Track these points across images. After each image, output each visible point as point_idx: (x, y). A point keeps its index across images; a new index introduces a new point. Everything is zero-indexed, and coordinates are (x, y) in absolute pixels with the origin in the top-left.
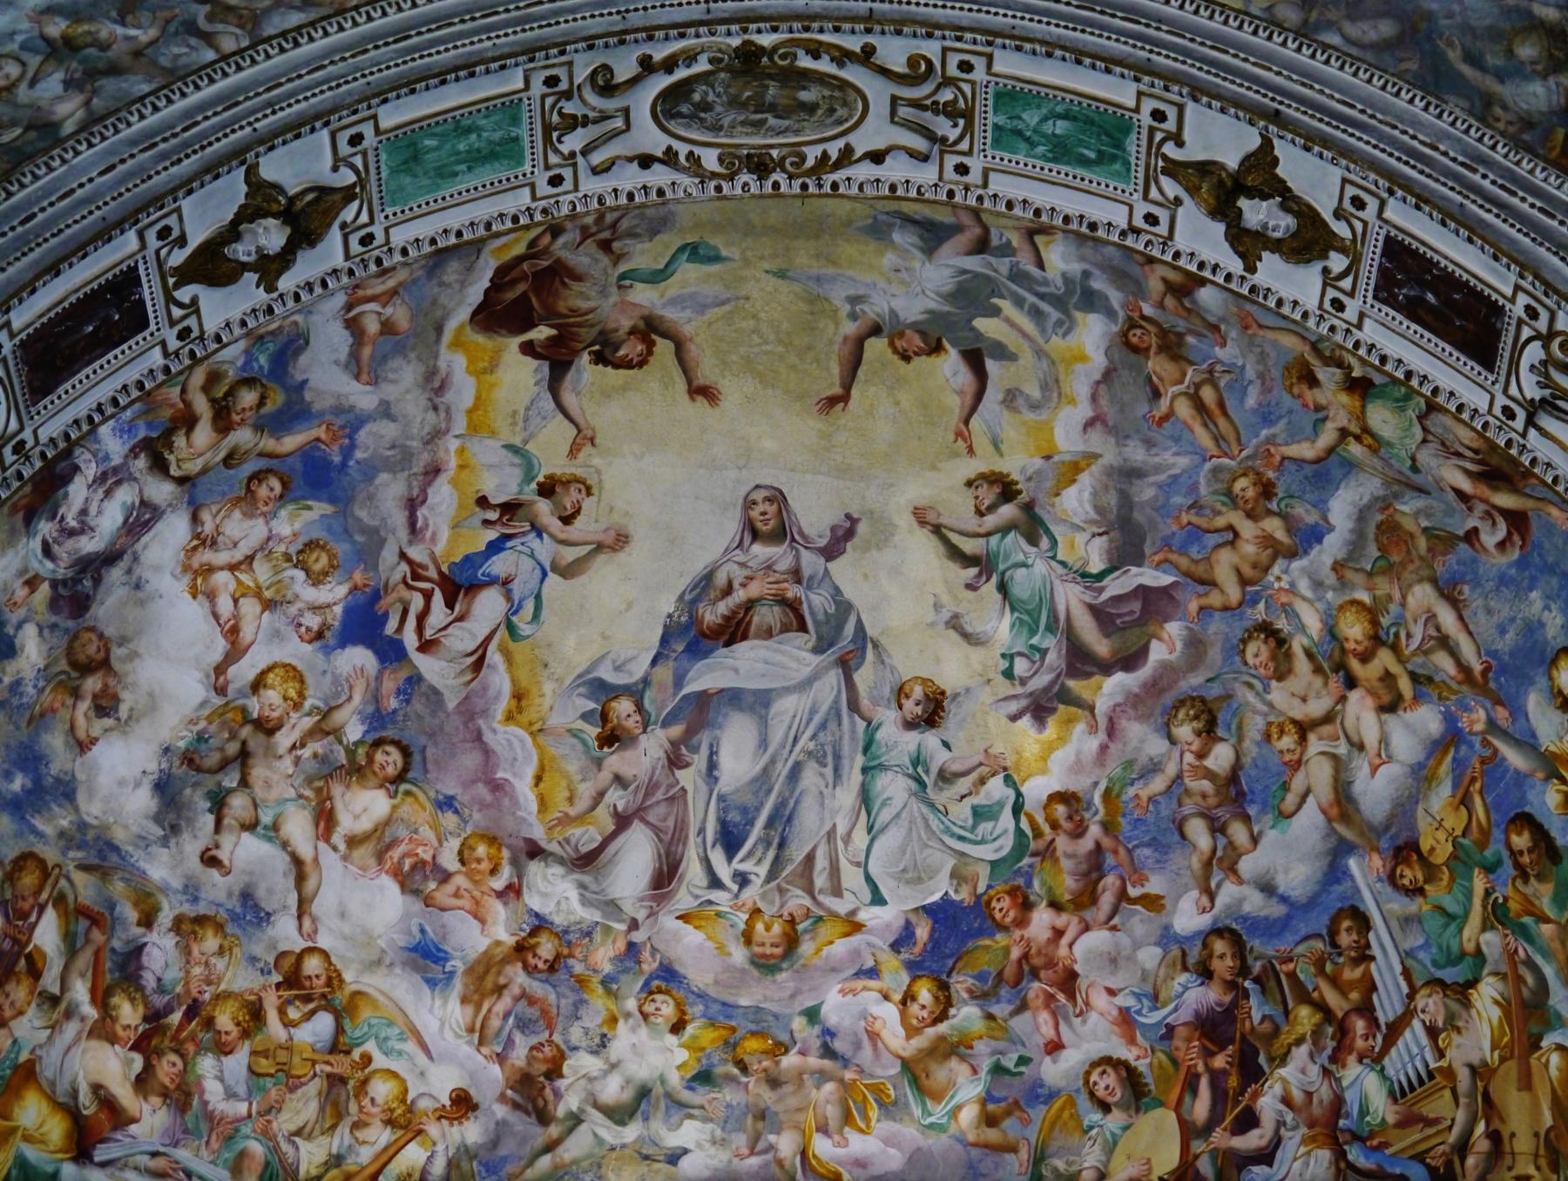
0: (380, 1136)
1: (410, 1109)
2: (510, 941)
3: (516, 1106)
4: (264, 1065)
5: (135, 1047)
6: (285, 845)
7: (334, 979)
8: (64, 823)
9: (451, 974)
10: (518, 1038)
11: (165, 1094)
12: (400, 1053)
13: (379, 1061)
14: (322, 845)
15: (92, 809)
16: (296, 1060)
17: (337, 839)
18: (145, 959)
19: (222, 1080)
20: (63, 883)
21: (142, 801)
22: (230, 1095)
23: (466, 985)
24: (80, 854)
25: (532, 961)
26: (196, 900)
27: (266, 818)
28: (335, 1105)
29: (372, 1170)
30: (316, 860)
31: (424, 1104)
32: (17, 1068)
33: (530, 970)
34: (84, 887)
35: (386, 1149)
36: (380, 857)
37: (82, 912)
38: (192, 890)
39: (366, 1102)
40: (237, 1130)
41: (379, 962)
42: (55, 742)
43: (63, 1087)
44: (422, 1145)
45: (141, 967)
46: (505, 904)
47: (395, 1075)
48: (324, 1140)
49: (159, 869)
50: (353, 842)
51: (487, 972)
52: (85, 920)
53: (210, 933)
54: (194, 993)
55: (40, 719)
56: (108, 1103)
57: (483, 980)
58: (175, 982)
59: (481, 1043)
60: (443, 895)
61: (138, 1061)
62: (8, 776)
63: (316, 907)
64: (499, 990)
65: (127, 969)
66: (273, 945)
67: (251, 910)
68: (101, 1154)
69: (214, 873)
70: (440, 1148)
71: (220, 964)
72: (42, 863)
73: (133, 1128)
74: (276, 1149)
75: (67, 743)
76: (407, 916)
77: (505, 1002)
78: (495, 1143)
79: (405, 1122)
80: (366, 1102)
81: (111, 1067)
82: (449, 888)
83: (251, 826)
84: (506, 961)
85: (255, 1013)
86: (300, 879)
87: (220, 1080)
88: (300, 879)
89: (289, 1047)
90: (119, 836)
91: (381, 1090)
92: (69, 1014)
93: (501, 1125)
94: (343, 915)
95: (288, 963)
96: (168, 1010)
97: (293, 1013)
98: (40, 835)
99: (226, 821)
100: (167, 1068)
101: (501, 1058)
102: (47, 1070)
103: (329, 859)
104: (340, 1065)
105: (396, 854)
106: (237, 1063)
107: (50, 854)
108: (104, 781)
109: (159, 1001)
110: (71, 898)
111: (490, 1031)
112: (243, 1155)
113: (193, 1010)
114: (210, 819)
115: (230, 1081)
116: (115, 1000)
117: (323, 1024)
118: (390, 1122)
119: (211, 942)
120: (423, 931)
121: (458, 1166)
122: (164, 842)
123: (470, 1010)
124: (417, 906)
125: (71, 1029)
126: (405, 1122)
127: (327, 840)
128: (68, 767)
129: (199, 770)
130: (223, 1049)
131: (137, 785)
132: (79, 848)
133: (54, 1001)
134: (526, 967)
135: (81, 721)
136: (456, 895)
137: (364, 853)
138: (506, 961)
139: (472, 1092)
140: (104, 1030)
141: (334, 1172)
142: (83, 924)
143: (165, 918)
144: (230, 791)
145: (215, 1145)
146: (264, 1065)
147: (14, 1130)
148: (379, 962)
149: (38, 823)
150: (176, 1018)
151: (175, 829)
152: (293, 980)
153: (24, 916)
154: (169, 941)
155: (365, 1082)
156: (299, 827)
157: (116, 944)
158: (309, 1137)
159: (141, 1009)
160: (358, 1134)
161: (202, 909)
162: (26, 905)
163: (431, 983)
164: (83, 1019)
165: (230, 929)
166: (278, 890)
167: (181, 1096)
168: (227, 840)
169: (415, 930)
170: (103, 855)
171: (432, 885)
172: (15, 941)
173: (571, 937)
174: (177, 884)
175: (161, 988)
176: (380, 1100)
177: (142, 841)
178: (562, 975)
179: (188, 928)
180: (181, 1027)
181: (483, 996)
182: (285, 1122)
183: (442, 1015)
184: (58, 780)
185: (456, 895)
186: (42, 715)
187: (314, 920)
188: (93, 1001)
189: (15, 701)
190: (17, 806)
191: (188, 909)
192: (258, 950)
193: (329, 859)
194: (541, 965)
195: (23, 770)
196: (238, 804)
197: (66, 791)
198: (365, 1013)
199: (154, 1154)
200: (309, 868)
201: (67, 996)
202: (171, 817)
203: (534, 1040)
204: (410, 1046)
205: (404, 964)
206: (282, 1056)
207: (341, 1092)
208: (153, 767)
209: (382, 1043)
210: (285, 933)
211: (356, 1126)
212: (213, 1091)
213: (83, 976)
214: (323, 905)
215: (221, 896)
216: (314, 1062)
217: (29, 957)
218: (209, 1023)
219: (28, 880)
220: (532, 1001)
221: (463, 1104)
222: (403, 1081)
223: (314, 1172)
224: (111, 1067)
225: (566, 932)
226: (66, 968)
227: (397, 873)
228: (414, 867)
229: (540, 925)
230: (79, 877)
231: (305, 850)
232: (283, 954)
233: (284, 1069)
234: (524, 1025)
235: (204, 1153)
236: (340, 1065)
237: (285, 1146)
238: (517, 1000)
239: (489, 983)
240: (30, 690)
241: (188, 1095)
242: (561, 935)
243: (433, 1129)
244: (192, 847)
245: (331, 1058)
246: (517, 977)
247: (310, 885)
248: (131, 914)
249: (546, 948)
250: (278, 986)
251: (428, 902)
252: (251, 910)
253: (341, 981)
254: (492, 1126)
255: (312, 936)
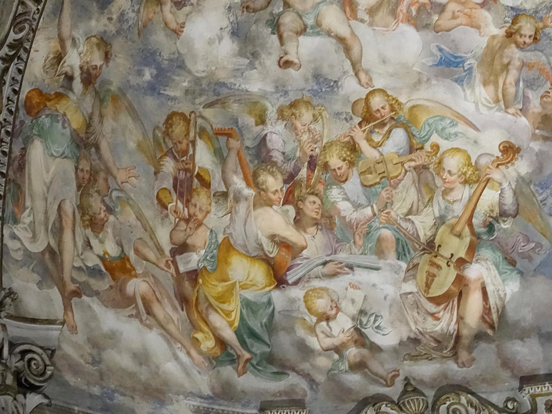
0: (463, 193)
1: (477, 168)
2: (501, 32)
3: (546, 139)
4: (371, 178)
5: (286, 202)
6: (329, 33)
7: (394, 105)
8: (185, 84)
9: (470, 70)
10: (530, 94)
11: (316, 224)
12: (456, 135)
13: (444, 145)
14: (353, 22)
15: (199, 68)
16: (390, 166)
17: (362, 14)
18: (269, 145)
19: (348, 199)
20: (199, 121)
21: (227, 47)
22: (357, 206)
23: (482, 74)
24: (203, 99)
25: (520, 40)
26: (286, 93)
27: (310, 21)
28: (427, 185)
29: (467, 216)
30: (353, 33)
31: (483, 161)
32: (219, 247)
33: (521, 47)
34: (214, 118)
35: (470, 200)
36: (394, 13)
37: (219, 133)
38: (281, 88)
39: (446, 175)
40: (370, 227)
41: (419, 82)
42: (159, 38)
43: (252, 245)
44: (492, 188)
45: (269, 151)
46: (489, 10)
47: (458, 150)
48: (428, 210)
49: (255, 84)
50: (372, 11)
51: (493, 60)
52: (221, 138)
53: (303, 110)
54: (309, 153)
55: (144, 29)
56: (284, 244)
57: (493, 64)
58: (294, 150)
59: (507, 107)
60: (445, 21)
61: (291, 210)
62: (140, 73)
63: (365, 64)
64: (506, 67)
65: (261, 152)
66: (346, 99)
67: (324, 84)
68: (291, 277)
69: (291, 71)
70: (505, 185)
71: (317, 127)
72: (182, 115)
73: (305, 252)
74: (398, 229)
75: (167, 35)
76: (426, 45)
77: (513, 75)
78: (539, 169)
79: (476, 178)
80: (446, 175)
81: (274, 221)
82: (448, 14)
83: (303, 31)
84: (503, 47)
85: (353, 148)
86: (347, 50)
87: (346, 200)
88: (347, 50)
89: (382, 161)
90: (222, 75)
91: (453, 163)
92: (237, 200)
93: (540, 155)
94: (384, 62)
95: (361, 107)
96: (297, 170)
97: (377, 138)
98: (173, 99)
99: (285, 35)
100: (311, 207)
101: (523, 111)
102: (238, 239)
103: (362, 30)
104: (420, 158)
105: (403, 7)
106: (353, 185)
107: (185, 108)
108: (199, 46)
109: (289, 167)
110: (209, 129)
111: (510, 97)
112: (379, 240)
113: (312, 164)
114: (275, 37)
115: (355, 198)
116: (262, 178)
117: (399, 135)
118: (466, 182)
119: (306, 115)
120: (441, 50)
121: (522, 193)
122: (252, 66)
123: (491, 88)
124: (430, 35)
125: (242, 208)
126: (476, 178)
127: (356, 18)
128: (174, 49)
129: (255, 11)
130: (341, 180)
131: (220, 39)
132: (200, 95)
133: (225, 195)
134: (518, 46)
135: (169, 17)
136: (454, 17)
137: (382, 15)
138: (503, 47)
139: (512, 141)
140: (263, 200)
141: (442, 228)
142: (223, 139)
143: (272, 113)
144: (280, 15)
145: (360, 242)
146: (371, 178)
147: (234, 284)
148: (419, 82)
149: (170, 92)
150: (304, 172)
151: (255, 55)
152: (368, 117)
153: (185, 153)
154: (280, 127)
155: (440, 163)
156: (333, 18)
157: (248, 143)
158: (418, 213)
159: (280, 177)
160: (449, 198)
161: (292, 97)
162: (183, 146)
163: (459, 81)
164: (246, 199)
165: (315, 102)
166: (336, 63)
167: (327, 221)
168: (291, 47)
169: (435, 51)
170: (217, 92)
171: (435, 17)
172: (186, 170)
173: (541, 14)
174: (270, 88)
175: (287, 158)
176: (454, 171)
177: (238, 72)
178: (544, 42)
179: (289, 112)
180: (309, 179)
181: (497, 76)
182: (398, 210)
183: (474, 100)
184: (171, 60)
185: (454, 17)
186: (145, 26)
187: (367, 72)
188: (248, 185)
189: (125, 27)
190: (153, 88)
191: (284, 101)
192: (338, 107)
193: (362, 30)
194: (528, 40)
195: (148, 65)
196: (289, 21)
197: (179, 64)
198: (423, 118)
199: (325, 264)
200: (350, 41)
201: (231, 189)
202: (250, 48)
203: (542, 91)
204: (461, 128)
205: (436, 76)
206: (381, 168)
207: (427, 177)
208: (225, 23)
209: (441, 133)
210: (352, 88)
211: (446, 192)
212: (344, 207)
213: (235, 172)
214: (369, 59)
215: (301, 84)
216: (402, 164)
217: (199, 176)
218: (326, 166)
219: (178, 129)
220: (530, 66)
221: (510, 150)
222: (465, 152)
223: (429, 234)
224: (274, 221)
225: (536, 12)
226: (223, 172)
227: (410, 20)
228: (419, 10)
229: (517, 14)
230: (208, 113)
231: (343, 31)
232: (355, 103)
233: (384, 176)
234: (531, 84)
235: (355, 250)
236: (420, 158)
237: (404, 225)
238: (520, 69)
239: (497, 66)
240: (132, 15)
241: (331, 217)
242: (534, 14)
243: (496, 175)
244: (270, 61)
245: (413, 156)
246: (515, 54)
247: (355, 51)
248: (250, 120)
249: (527, 28)
250: (360, 124)
251: (437, 29)
252: (324, 84)
253: (400, 104)
254: (534, 158)
255: (370, 83)
